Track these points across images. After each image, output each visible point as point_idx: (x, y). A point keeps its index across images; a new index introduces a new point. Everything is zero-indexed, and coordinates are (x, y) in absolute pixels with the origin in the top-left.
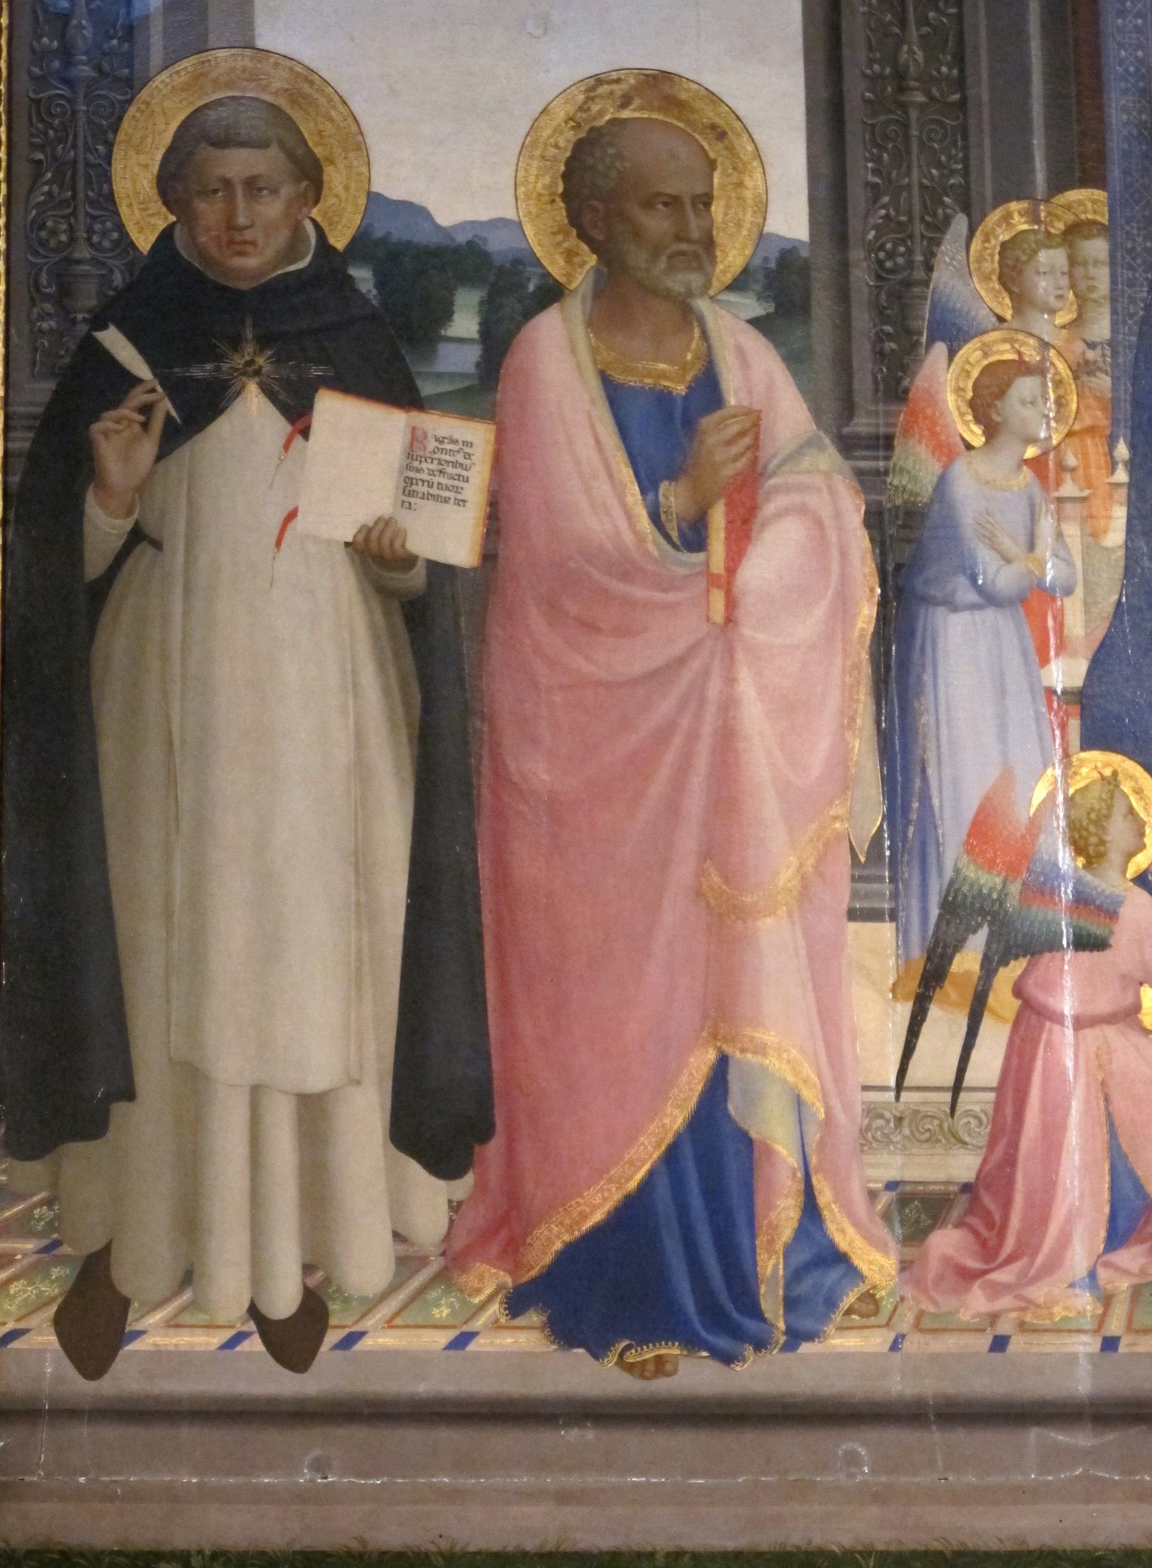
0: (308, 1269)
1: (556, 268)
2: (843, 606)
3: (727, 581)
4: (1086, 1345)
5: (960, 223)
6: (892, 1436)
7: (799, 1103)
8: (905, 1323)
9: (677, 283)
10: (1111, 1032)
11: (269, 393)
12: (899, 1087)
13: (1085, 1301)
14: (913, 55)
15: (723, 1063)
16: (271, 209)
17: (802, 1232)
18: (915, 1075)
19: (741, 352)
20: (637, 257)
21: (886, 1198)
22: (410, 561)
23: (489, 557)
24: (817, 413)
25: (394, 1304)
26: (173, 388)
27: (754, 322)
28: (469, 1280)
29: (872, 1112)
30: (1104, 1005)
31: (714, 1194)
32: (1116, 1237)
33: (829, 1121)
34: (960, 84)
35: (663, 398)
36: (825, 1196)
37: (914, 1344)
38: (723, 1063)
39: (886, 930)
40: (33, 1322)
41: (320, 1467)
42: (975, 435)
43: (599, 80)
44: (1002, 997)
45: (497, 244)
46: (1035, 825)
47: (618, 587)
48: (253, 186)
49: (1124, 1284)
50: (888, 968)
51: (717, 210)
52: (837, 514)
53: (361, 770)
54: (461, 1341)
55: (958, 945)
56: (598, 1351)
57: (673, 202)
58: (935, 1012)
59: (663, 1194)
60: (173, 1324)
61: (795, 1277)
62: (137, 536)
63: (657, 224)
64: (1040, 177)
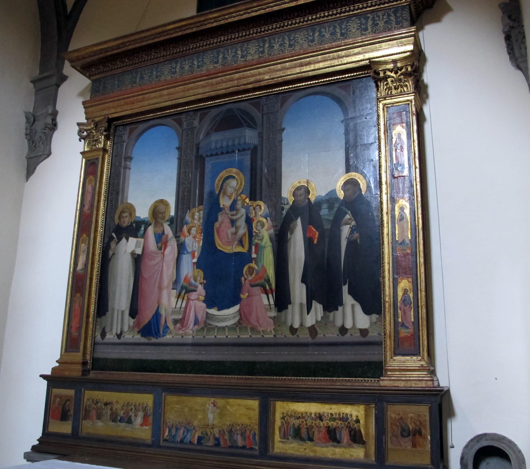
0: (121, 329)
1: (151, 222)
3: (163, 253)
4: (191, 337)
5: (189, 211)
6: (172, 347)
8: (174, 334)
9: (161, 222)
10: (196, 301)
11: (125, 238)
13: (191, 332)
14: (186, 193)
15: (158, 307)
16: (127, 219)
17: (165, 324)
18: (177, 307)
19: (167, 229)
20: (159, 220)
23: (143, 253)
24: (173, 233)
25: (127, 333)
26: (118, 238)
27: (168, 225)
29: (172, 311)
32: (195, 324)
34: (190, 196)
35: (159, 234)
36: (167, 320)
37: (175, 337)
39: (175, 291)
41: (121, 350)
42: (188, 235)
43: (156, 201)
44: (186, 298)
45: (146, 220)
46: (190, 278)
47: (152, 254)
48: (126, 217)
50: (175, 295)
51: (166, 213)
52: (174, 245)
53: (130, 276)
55: (182, 292)
57: (162, 213)
58: (179, 299)
59: (152, 321)
61: (164, 329)
63: (160, 216)
64: (197, 205)
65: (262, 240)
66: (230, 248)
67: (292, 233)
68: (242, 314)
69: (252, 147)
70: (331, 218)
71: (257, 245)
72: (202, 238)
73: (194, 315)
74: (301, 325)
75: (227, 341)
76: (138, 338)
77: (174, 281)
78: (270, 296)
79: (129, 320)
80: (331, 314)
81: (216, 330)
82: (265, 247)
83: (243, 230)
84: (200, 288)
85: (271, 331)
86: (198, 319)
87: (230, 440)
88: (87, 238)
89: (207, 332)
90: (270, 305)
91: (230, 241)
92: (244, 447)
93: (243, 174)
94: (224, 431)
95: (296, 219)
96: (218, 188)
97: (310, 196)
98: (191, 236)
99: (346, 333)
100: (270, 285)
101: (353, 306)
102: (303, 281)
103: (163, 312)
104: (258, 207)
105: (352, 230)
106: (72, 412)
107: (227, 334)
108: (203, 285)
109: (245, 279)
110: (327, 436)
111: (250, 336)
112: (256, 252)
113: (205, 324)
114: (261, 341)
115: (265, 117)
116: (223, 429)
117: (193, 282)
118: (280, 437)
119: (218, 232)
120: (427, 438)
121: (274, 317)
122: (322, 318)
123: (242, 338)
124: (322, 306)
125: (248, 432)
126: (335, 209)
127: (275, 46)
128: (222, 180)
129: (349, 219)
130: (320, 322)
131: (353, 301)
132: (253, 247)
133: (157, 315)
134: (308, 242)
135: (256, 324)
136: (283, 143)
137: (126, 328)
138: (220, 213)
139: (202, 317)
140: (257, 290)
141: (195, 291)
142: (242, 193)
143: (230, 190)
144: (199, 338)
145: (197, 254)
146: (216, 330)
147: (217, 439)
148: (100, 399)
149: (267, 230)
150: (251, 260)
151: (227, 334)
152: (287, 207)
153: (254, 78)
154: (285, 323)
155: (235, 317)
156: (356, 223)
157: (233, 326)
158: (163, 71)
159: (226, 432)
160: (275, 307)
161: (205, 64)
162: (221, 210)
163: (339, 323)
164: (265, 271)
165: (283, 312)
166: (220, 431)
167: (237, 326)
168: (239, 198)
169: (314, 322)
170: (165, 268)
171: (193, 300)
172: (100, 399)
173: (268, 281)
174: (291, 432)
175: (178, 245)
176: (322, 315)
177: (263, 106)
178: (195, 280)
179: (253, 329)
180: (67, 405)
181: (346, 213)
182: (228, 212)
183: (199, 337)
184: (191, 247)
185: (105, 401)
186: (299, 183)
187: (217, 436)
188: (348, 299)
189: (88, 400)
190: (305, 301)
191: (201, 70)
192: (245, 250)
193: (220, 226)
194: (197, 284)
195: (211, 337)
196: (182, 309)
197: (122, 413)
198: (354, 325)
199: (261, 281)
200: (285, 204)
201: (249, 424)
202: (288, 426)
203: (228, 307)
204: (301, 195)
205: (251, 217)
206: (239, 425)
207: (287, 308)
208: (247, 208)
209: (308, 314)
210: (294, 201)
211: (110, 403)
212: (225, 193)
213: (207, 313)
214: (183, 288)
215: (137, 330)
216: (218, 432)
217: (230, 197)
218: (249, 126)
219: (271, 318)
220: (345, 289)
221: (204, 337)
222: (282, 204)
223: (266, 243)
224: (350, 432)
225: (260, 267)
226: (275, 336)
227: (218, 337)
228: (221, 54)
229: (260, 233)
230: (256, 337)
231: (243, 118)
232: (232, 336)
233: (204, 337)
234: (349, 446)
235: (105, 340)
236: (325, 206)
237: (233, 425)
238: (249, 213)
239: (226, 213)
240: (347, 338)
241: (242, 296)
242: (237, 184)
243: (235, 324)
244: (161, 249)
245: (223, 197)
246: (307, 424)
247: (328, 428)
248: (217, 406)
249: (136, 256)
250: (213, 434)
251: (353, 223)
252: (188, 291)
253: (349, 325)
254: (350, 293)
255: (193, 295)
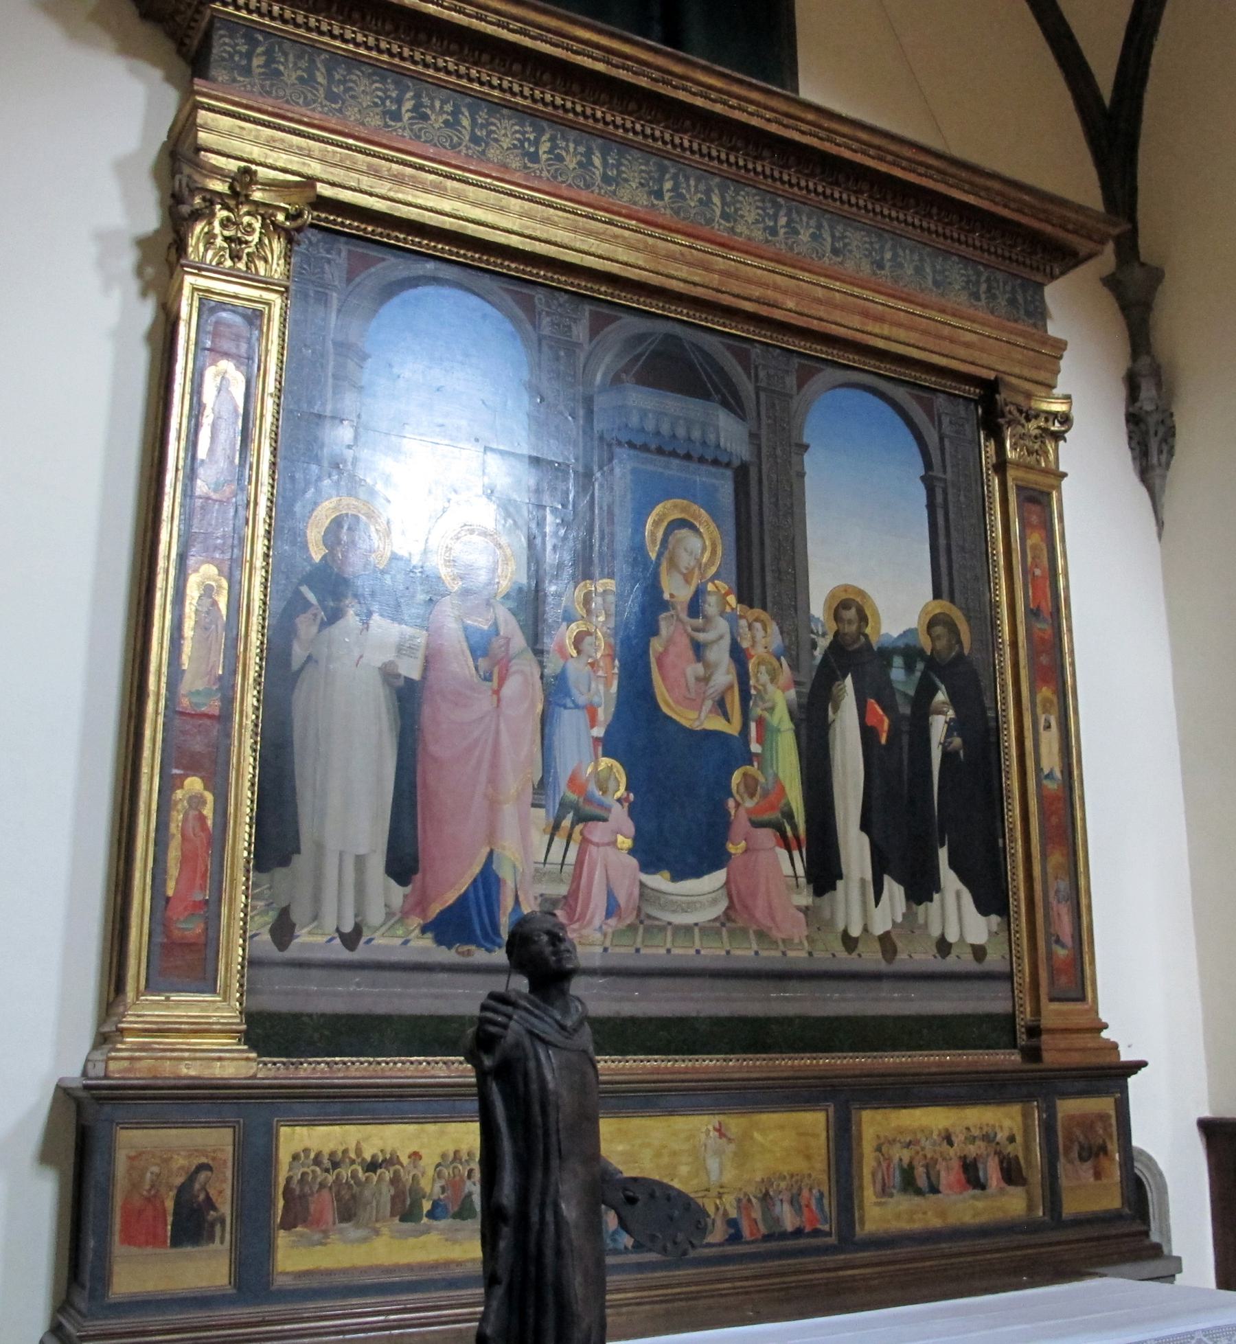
0: (356, 916)
2: (533, 705)
3: (497, 692)
4: (599, 950)
7: (514, 867)
12: (545, 863)
13: (598, 936)
15: (491, 853)
21: (539, 900)
22: (399, 675)
23: (424, 677)
24: (527, 641)
25: (383, 929)
28: (409, 921)
29: (537, 870)
30: (606, 840)
31: (488, 897)
32: (609, 914)
33: (523, 873)
36: (521, 898)
38: (491, 853)
39: (542, 812)
40: (262, 931)
42: (574, 653)
44: (576, 835)
46: (588, 780)
49: (610, 930)
54: (406, 942)
55: (564, 817)
56: (450, 946)
58: (556, 839)
59: (472, 896)
60: (310, 933)
62: (309, 658)
65: (771, 710)
66: (693, 715)
67: (836, 709)
68: (734, 892)
69: (736, 463)
70: (912, 692)
71: (761, 722)
72: (616, 671)
73: (604, 887)
74: (866, 929)
75: (698, 963)
76: (424, 947)
77: (536, 783)
78: (796, 854)
79: (387, 889)
80: (922, 908)
81: (669, 933)
82: (779, 731)
83: (724, 676)
84: (619, 815)
85: (801, 943)
86: (616, 901)
87: (765, 1220)
88: (225, 584)
89: (643, 941)
90: (796, 877)
91: (693, 695)
92: (798, 1233)
93: (718, 527)
94: (749, 1200)
95: (845, 676)
96: (654, 542)
97: (868, 630)
98: (584, 659)
99: (949, 953)
100: (795, 828)
101: (958, 895)
102: (865, 826)
103: (505, 872)
104: (758, 625)
105: (951, 729)
106: (226, 1209)
107: (697, 945)
108: (626, 805)
109: (738, 805)
110: (963, 1177)
111: (757, 953)
112: (760, 740)
113: (638, 915)
114: (779, 966)
115: (763, 396)
116: (746, 1194)
117: (598, 794)
118: (875, 1193)
119: (660, 666)
120: (1114, 1159)
121: (807, 908)
122: (904, 915)
123: (738, 957)
124: (902, 889)
125: (805, 1193)
126: (918, 674)
127: (802, 231)
128: (665, 524)
129: (944, 703)
130: (901, 925)
131: (959, 885)
132: (753, 726)
133: (488, 881)
134: (868, 734)
135: (767, 922)
136: (807, 479)
137: (375, 915)
138: (663, 615)
139: (631, 895)
140: (766, 836)
141: (605, 820)
142: (716, 576)
143: (685, 561)
144: (622, 954)
145: (604, 715)
146: (669, 933)
147: (732, 1223)
148: (345, 1152)
149: (784, 690)
150: (749, 758)
151: (697, 945)
152: (824, 643)
153: (761, 290)
154: (831, 923)
155: (714, 902)
156: (956, 712)
157: (712, 924)
158: (494, 132)
159: (754, 1200)
160: (809, 882)
161: (626, 180)
162: (665, 606)
163: (935, 932)
164: (782, 789)
165: (827, 896)
166: (739, 1201)
167: (723, 925)
168: (710, 587)
169: (889, 927)
170: (505, 739)
171: (597, 845)
172: (345, 1152)
173: (789, 816)
174: (897, 1179)
175: (542, 677)
176: (904, 910)
177: (756, 368)
178: (605, 792)
179: (762, 935)
180: (197, 1186)
181: (935, 690)
182: (684, 616)
183: (623, 950)
184: (584, 689)
185: (369, 1158)
186: (846, 591)
187: (733, 1214)
188: (949, 878)
189: (295, 1157)
190: (869, 876)
191: (614, 193)
192: (733, 729)
193: (666, 650)
194: (610, 800)
195: (656, 952)
196: (568, 870)
197: (437, 1189)
198: (961, 935)
199: (775, 815)
200: (817, 634)
201: (806, 1172)
202: (889, 1165)
203: (698, 874)
204: (850, 622)
205: (745, 644)
206: (785, 1177)
207: (834, 888)
208: (733, 620)
209: (877, 904)
210: (836, 634)
211: (392, 1161)
212: (673, 564)
213: (642, 885)
214: (564, 806)
215: (415, 922)
216: (735, 1204)
217: (687, 579)
218: (725, 404)
219: (799, 908)
220: (943, 854)
221: (638, 950)
222: (812, 632)
223: (781, 721)
224: (1001, 1162)
225: (770, 778)
226: (810, 954)
227: (675, 951)
228: (667, 176)
229: (765, 690)
230: (770, 957)
231: (709, 377)
232: (713, 952)
233: (638, 950)
234: (1002, 1191)
235: (293, 951)
236: (898, 661)
237: (769, 1179)
238: (739, 634)
239: (679, 620)
240: (951, 963)
241: (731, 848)
242: (704, 549)
243: (716, 920)
244: (488, 678)
245: (669, 571)
246: (925, 1156)
247: (964, 1159)
248: (729, 1135)
249: (401, 682)
250: (721, 1211)
251: (951, 714)
252: (582, 818)
253: (952, 937)
254: (953, 865)
255: (598, 832)
